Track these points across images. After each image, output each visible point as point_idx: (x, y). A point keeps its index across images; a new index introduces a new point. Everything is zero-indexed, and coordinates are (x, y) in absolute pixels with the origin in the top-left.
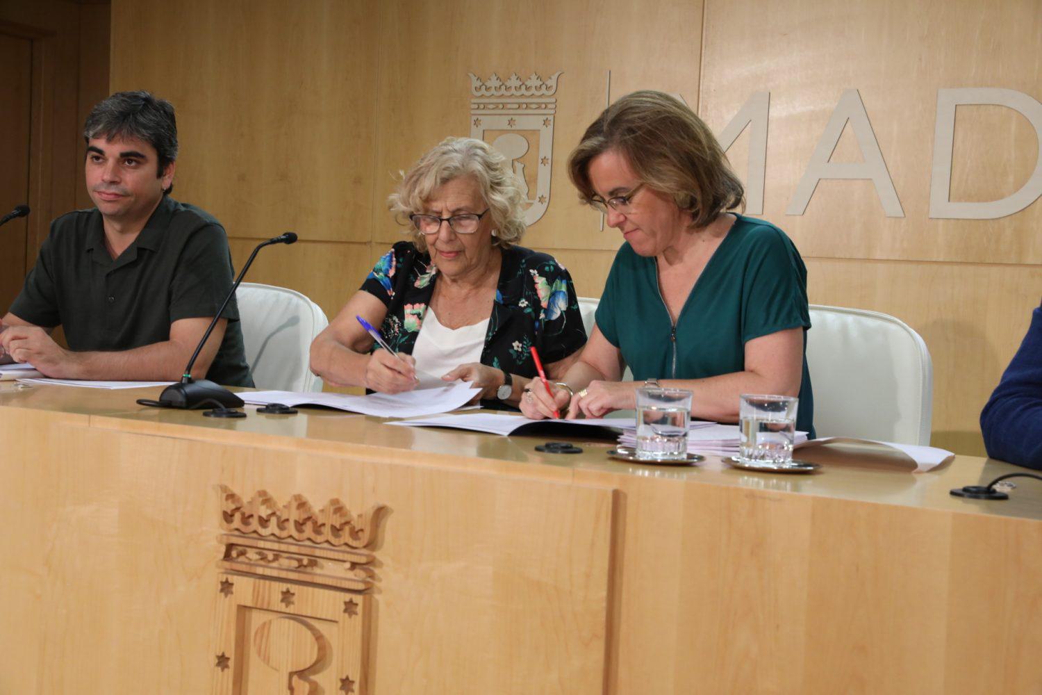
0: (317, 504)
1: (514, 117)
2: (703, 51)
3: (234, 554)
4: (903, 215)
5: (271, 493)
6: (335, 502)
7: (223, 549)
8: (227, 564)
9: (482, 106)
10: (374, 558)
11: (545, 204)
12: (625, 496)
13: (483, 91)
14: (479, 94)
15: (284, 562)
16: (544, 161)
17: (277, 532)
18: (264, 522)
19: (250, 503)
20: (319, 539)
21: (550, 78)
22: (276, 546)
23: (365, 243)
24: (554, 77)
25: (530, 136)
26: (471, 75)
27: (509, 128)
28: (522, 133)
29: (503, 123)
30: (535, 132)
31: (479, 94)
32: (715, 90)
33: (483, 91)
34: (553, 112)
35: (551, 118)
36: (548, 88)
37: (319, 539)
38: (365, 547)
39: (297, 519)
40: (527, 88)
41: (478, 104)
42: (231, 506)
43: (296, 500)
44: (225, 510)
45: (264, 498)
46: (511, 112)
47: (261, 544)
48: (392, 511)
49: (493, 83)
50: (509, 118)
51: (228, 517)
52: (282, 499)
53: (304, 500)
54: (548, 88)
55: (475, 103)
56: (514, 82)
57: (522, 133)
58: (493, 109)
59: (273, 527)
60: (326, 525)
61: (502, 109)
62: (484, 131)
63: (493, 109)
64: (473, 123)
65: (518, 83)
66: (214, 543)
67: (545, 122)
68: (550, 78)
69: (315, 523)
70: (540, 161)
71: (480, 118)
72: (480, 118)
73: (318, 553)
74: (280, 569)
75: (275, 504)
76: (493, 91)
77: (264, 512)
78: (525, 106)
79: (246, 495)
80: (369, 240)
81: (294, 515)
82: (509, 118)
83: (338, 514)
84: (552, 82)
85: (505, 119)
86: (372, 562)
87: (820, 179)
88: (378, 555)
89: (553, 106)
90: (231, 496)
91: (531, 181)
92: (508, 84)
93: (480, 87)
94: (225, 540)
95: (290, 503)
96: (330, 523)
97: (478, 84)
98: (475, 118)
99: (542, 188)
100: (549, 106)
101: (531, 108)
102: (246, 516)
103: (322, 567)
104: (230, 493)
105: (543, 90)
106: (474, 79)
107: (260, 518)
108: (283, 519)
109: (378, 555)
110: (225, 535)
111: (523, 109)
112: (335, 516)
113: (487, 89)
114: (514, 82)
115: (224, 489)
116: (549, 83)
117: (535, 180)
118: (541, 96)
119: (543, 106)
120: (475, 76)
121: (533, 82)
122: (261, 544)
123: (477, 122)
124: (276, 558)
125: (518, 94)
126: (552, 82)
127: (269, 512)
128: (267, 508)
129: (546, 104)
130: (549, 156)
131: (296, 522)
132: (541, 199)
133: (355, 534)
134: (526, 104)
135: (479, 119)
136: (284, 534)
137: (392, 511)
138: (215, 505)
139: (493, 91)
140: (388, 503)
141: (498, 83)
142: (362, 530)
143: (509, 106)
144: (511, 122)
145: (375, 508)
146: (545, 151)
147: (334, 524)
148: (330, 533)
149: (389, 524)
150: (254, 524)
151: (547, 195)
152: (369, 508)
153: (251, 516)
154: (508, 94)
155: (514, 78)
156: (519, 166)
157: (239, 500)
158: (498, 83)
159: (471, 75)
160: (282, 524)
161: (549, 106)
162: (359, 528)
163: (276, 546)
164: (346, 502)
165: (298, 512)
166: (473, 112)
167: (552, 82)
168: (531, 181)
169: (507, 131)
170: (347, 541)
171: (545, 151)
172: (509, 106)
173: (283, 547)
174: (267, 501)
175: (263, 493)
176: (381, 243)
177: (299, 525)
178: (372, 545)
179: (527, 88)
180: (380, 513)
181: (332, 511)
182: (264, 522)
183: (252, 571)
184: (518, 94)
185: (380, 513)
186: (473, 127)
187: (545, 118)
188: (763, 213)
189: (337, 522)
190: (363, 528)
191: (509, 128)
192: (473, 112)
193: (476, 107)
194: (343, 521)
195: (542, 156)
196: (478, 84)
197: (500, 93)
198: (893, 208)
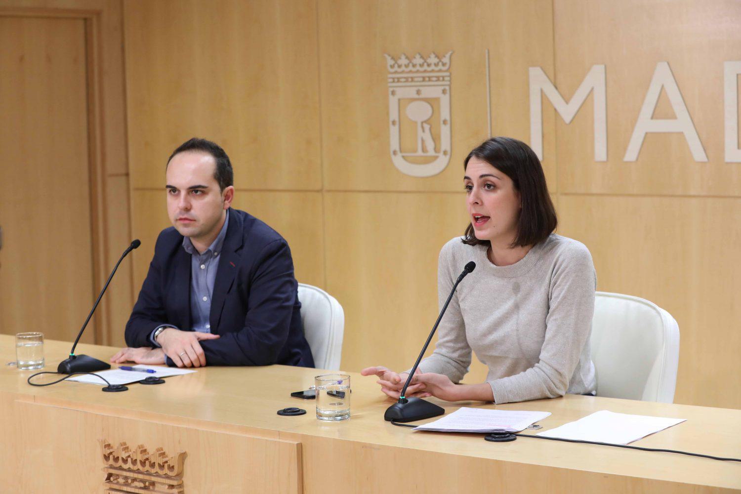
0: (152, 450)
1: (421, 88)
3: (112, 479)
4: (706, 160)
6: (158, 450)
7: (106, 476)
8: (109, 485)
9: (396, 80)
11: (448, 157)
13: (396, 68)
14: (393, 70)
15: (136, 484)
16: (445, 122)
18: (125, 461)
24: (448, 56)
25: (433, 102)
28: (426, 100)
29: (411, 92)
30: (437, 100)
31: (393, 70)
33: (396, 68)
34: (448, 83)
35: (447, 88)
40: (429, 65)
41: (393, 79)
43: (140, 448)
45: (124, 447)
46: (418, 84)
49: (403, 61)
51: (107, 458)
52: (133, 447)
53: (145, 448)
54: (444, 64)
55: (390, 78)
57: (426, 100)
59: (129, 465)
62: (399, 100)
67: (444, 92)
69: (150, 462)
70: (442, 122)
71: (395, 89)
74: (136, 487)
77: (124, 455)
79: (116, 444)
81: (139, 457)
82: (416, 89)
83: (161, 457)
84: (446, 60)
86: (181, 486)
87: (646, 133)
90: (108, 446)
91: (436, 139)
95: (136, 450)
97: (392, 62)
98: (391, 89)
99: (445, 144)
101: (433, 81)
102: (115, 457)
104: (107, 443)
105: (440, 67)
106: (389, 58)
107: (123, 459)
108: (134, 459)
109: (186, 480)
110: (106, 468)
111: (426, 81)
112: (159, 458)
113: (399, 66)
114: (418, 60)
117: (439, 138)
118: (440, 71)
120: (389, 55)
121: (433, 60)
122: (125, 474)
123: (393, 93)
124: (134, 480)
126: (446, 60)
127: (127, 455)
128: (126, 452)
129: (443, 77)
130: (448, 118)
131: (141, 461)
132: (445, 153)
133: (171, 468)
138: (99, 452)
139: (403, 68)
144: (418, 92)
145: (179, 454)
146: (445, 114)
149: (188, 461)
150: (120, 462)
151: (448, 149)
153: (118, 457)
154: (414, 69)
156: (427, 127)
157: (112, 448)
159: (386, 56)
160: (134, 462)
164: (165, 450)
168: (436, 139)
171: (445, 114)
173: (136, 476)
174: (126, 449)
176: (329, 191)
177: (143, 463)
178: (180, 475)
179: (429, 65)
181: (158, 455)
182: (125, 461)
183: (121, 489)
185: (183, 456)
186: (391, 97)
187: (443, 88)
189: (161, 461)
193: (391, 80)
195: (442, 118)
198: (699, 155)
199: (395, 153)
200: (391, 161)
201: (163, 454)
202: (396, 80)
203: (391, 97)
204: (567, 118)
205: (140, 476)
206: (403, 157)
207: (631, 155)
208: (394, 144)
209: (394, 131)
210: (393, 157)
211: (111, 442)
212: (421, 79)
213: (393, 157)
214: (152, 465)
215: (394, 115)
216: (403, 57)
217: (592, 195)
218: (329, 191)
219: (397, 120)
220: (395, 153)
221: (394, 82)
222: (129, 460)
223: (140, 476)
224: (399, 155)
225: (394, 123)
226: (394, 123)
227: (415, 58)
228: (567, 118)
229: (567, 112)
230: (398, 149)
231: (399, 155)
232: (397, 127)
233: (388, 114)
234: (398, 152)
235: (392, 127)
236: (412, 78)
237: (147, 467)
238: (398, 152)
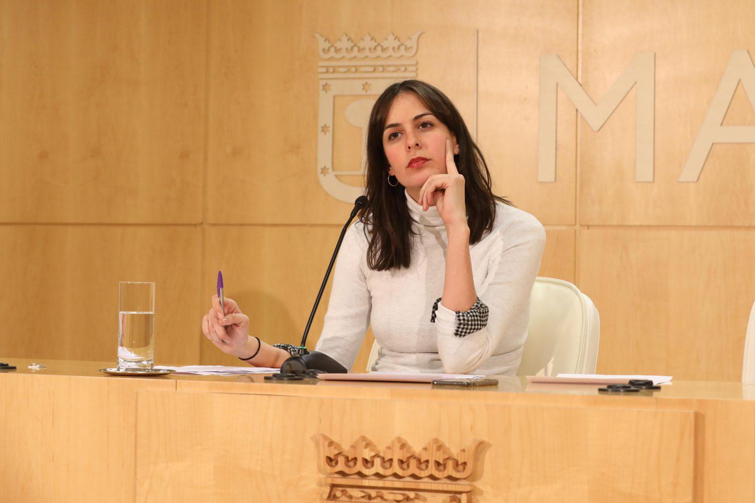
1: (369, 82)
2: (581, 9)
5: (369, 437)
6: (436, 441)
7: (328, 490)
9: (331, 70)
10: (475, 487)
12: (703, 416)
17: (381, 471)
19: (353, 447)
20: (423, 474)
21: (410, 38)
22: (380, 483)
23: (195, 225)
26: (317, 35)
27: (363, 92)
32: (595, 51)
33: (332, 53)
36: (406, 49)
37: (423, 474)
38: (464, 479)
39: (401, 458)
41: (327, 67)
42: (332, 453)
44: (329, 455)
46: (367, 75)
47: (366, 483)
48: (490, 445)
49: (344, 44)
50: (364, 82)
51: (330, 460)
53: (403, 442)
54: (406, 49)
56: (367, 43)
58: (345, 72)
59: (378, 468)
60: (430, 462)
61: (356, 71)
62: (334, 97)
63: (345, 72)
64: (321, 88)
65: (373, 44)
66: (314, 486)
68: (410, 38)
69: (419, 461)
71: (329, 82)
72: (329, 82)
73: (422, 486)
75: (375, 447)
76: (343, 53)
77: (367, 454)
78: (381, 69)
80: (200, 221)
81: (397, 455)
85: (358, 84)
87: (713, 144)
88: (479, 484)
89: (414, 68)
90: (331, 443)
92: (361, 44)
93: (329, 48)
94: (330, 481)
95: (393, 443)
96: (434, 459)
97: (326, 45)
98: (323, 82)
100: (410, 68)
101: (389, 71)
103: (425, 500)
105: (402, 51)
109: (479, 484)
112: (438, 453)
113: (337, 51)
114: (367, 43)
115: (325, 437)
116: (408, 44)
119: (403, 69)
120: (322, 36)
121: (391, 43)
123: (326, 88)
125: (373, 55)
127: (373, 454)
134: (383, 66)
135: (328, 84)
136: (389, 472)
137: (490, 445)
140: (485, 439)
141: (349, 45)
142: (465, 463)
143: (362, 69)
147: (438, 460)
148: (433, 466)
152: (469, 443)
155: (367, 38)
158: (349, 45)
161: (410, 68)
162: (463, 461)
163: (380, 483)
164: (445, 440)
165: (401, 451)
166: (321, 76)
167: (412, 43)
169: (361, 96)
170: (451, 474)
172: (362, 69)
173: (388, 484)
175: (364, 438)
176: (214, 225)
180: (481, 447)
181: (435, 447)
184: (373, 55)
185: (481, 447)
186: (322, 93)
188: (556, 181)
190: (466, 461)
191: (363, 92)
192: (321, 76)
193: (324, 70)
194: (446, 457)
196: (326, 45)
197: (352, 55)
199: (324, 170)
200: (318, 183)
201: (440, 447)
202: (331, 70)
203: (322, 93)
204: (595, 124)
205: (398, 484)
206: (336, 176)
207: (690, 172)
208: (324, 158)
209: (324, 141)
210: (321, 176)
211: (335, 438)
212: (372, 69)
213: (321, 176)
214: (422, 463)
215: (325, 117)
216: (345, 39)
217: (629, 227)
218: (214, 225)
219: (330, 124)
220: (324, 170)
221: (327, 72)
222: (377, 461)
223: (398, 484)
224: (331, 174)
225: (324, 129)
226: (324, 129)
227: (363, 40)
228: (595, 124)
229: (594, 117)
230: (329, 165)
231: (331, 174)
232: (329, 135)
233: (316, 116)
234: (330, 170)
235: (321, 135)
236: (355, 67)
237: (413, 469)
238: (330, 170)
